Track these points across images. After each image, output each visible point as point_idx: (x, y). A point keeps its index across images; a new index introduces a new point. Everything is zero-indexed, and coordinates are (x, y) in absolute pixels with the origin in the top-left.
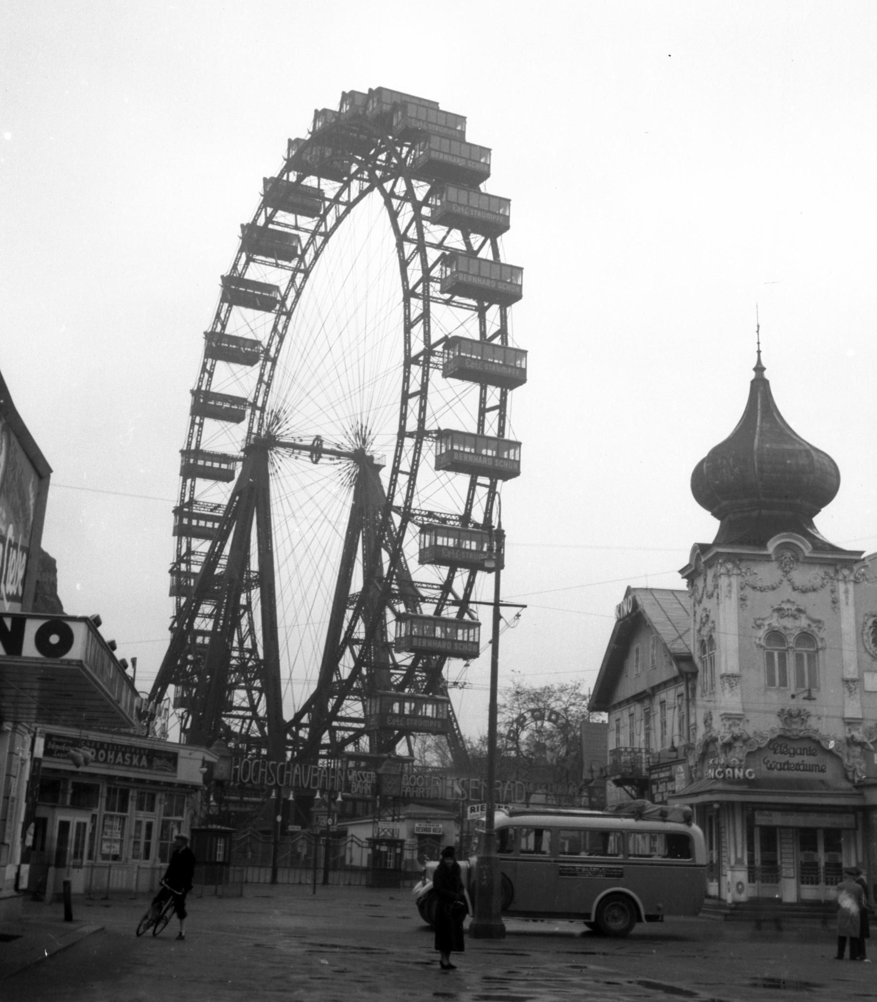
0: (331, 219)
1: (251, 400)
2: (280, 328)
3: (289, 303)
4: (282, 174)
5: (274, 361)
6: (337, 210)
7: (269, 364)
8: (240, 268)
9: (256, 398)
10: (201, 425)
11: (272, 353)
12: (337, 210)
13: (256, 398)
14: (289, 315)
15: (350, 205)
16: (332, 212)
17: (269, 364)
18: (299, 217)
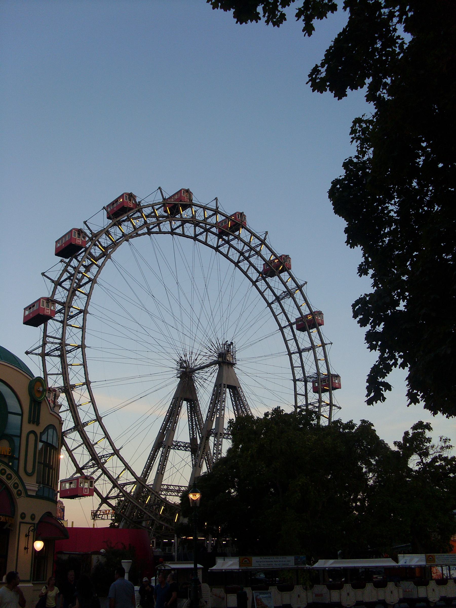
5: (290, 354)
11: (296, 357)
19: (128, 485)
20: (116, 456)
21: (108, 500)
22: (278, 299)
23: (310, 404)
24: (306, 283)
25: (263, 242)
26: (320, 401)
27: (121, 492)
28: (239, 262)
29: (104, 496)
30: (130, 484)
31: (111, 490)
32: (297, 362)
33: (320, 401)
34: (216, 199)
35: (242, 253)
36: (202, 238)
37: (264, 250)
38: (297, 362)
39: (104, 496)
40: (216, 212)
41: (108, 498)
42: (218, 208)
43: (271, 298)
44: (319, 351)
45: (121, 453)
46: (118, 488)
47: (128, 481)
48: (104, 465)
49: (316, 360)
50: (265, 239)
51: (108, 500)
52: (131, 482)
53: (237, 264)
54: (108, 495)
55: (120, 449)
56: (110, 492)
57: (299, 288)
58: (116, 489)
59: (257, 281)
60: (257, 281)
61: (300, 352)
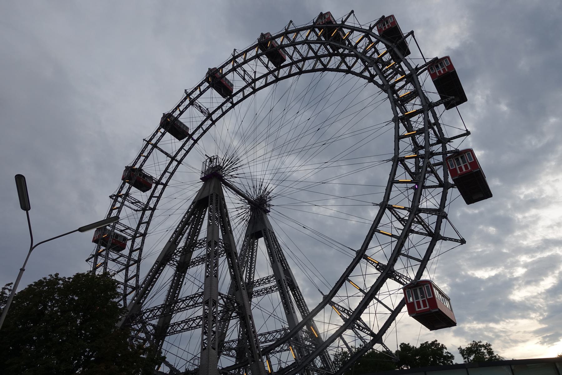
0: (283, 72)
1: (190, 132)
2: (224, 108)
3: (235, 99)
4: (278, 36)
5: (214, 122)
6: (290, 70)
7: (209, 122)
8: (225, 70)
9: (193, 133)
10: (163, 134)
11: (214, 117)
12: (290, 70)
13: (193, 133)
14: (233, 105)
15: (301, 72)
16: (286, 70)
17: (209, 122)
18: (270, 62)
19: (399, 216)
20: (367, 253)
21: (433, 231)
22: (173, 159)
23: (244, 79)
24: (144, 140)
25: (118, 196)
26: (234, 69)
27: (413, 221)
28: (150, 209)
29: (430, 239)
30: (397, 214)
31: (417, 233)
32: (219, 112)
33: (234, 69)
34: (87, 261)
35: (144, 210)
36: (135, 255)
37: (124, 192)
38: (219, 112)
39: (430, 239)
40: (97, 255)
41: (430, 234)
42: (93, 255)
43: (175, 163)
44: (193, 96)
45: (358, 247)
46: (410, 225)
47: (394, 219)
48: (386, 265)
49: (201, 93)
50: (114, 195)
51: (433, 231)
52: (392, 213)
53: (153, 210)
54: (426, 235)
55: (355, 251)
56: (422, 234)
57: (148, 142)
58: (413, 228)
59: (162, 184)
60: (162, 184)
61: (209, 116)
